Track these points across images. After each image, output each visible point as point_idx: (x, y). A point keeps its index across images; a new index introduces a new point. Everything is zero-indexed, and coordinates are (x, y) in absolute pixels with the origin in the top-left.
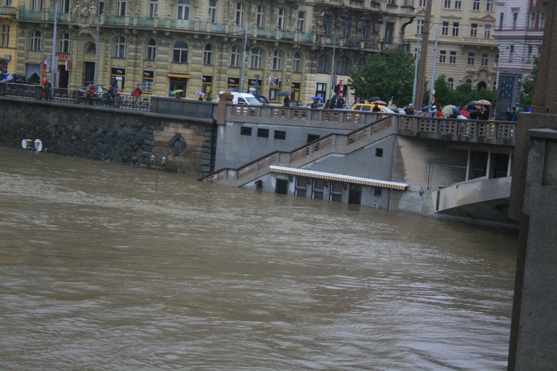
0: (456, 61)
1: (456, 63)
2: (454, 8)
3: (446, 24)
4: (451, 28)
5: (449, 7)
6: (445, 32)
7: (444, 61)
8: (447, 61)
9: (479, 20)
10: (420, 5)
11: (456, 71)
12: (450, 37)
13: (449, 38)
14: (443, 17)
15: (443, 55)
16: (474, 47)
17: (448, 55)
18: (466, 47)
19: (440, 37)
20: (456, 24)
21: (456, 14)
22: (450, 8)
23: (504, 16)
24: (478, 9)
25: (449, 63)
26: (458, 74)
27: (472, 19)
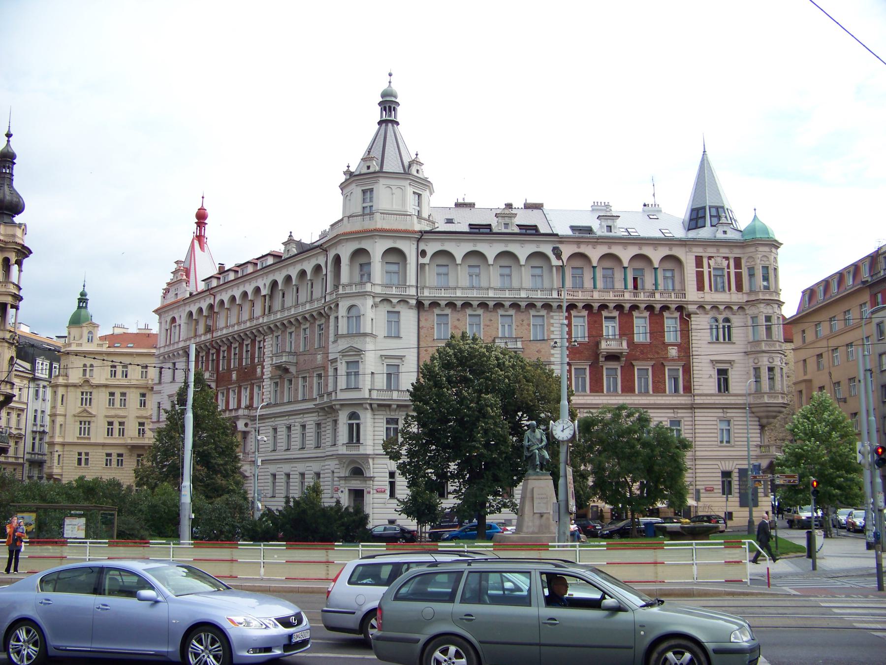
0: (124, 463)
1: (124, 467)
2: (119, 407)
3: (110, 423)
4: (116, 426)
5: (113, 405)
6: (110, 432)
7: (110, 465)
8: (114, 462)
9: (146, 418)
10: (82, 404)
11: (124, 475)
12: (115, 438)
13: (116, 439)
14: (107, 417)
15: (109, 458)
16: (142, 447)
17: (114, 458)
18: (133, 448)
19: (105, 438)
20: (121, 424)
21: (121, 413)
22: (115, 407)
23: (161, 405)
24: (144, 406)
25: (116, 466)
26: (126, 478)
27: (138, 417)
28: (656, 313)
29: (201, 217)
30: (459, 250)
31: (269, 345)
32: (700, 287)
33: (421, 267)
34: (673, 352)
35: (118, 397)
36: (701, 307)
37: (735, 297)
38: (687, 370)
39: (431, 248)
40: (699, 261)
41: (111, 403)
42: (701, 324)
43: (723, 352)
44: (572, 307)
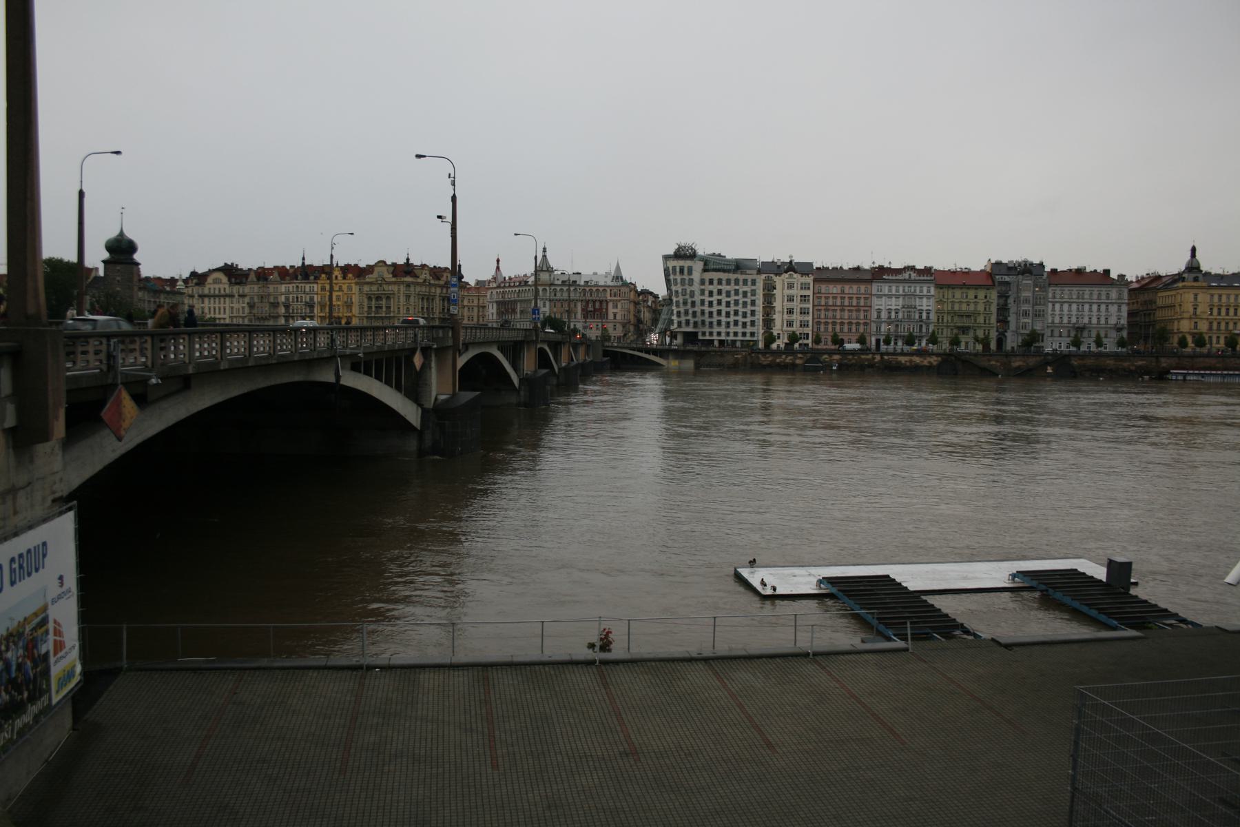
4: (471, 318)
28: (601, 302)
29: (498, 261)
30: (558, 288)
31: (519, 304)
32: (611, 296)
33: (550, 292)
34: (604, 310)
35: (471, 309)
36: (611, 300)
37: (617, 298)
38: (607, 314)
39: (553, 288)
40: (611, 290)
41: (469, 311)
42: (610, 305)
43: (615, 311)
44: (582, 300)
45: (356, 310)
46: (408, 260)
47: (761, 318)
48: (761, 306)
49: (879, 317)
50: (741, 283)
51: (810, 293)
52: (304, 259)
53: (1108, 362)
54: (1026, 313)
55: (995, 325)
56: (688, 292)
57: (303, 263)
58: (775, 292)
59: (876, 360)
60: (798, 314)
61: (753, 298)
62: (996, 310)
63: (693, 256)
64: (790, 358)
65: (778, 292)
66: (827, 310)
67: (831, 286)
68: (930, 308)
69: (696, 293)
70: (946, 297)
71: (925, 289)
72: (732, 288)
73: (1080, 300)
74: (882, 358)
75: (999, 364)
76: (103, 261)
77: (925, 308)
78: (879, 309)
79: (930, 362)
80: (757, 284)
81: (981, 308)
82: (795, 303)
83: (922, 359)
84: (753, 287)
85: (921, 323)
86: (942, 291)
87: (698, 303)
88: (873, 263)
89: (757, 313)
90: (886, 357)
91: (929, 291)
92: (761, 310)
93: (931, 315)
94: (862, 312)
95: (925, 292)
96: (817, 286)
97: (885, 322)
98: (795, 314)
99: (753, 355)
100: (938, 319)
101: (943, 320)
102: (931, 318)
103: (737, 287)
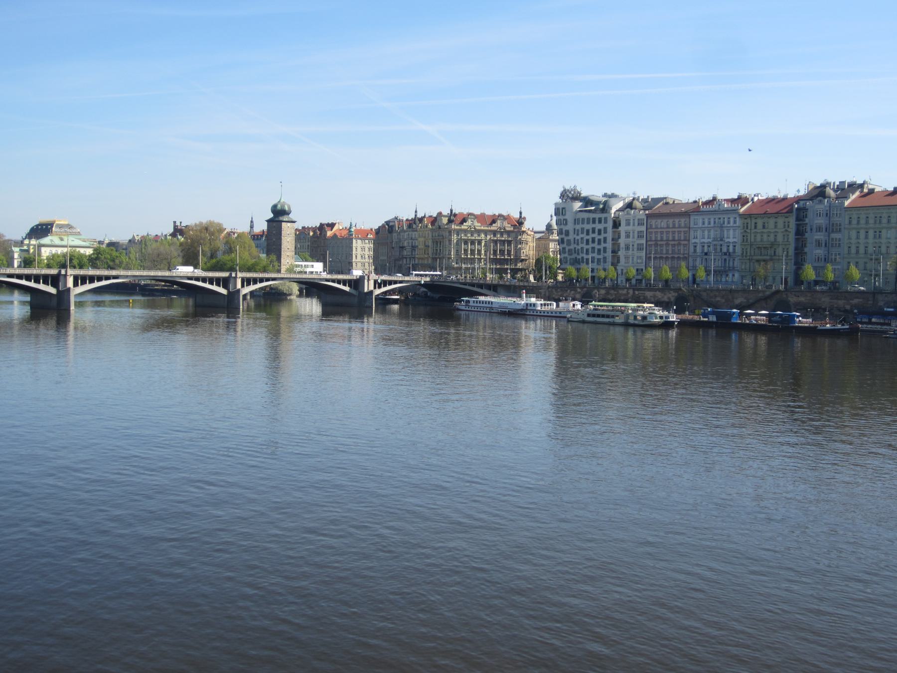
45: (430, 251)
46: (451, 211)
47: (611, 254)
48: (611, 242)
49: (695, 251)
50: (597, 222)
51: (643, 228)
52: (416, 212)
53: (823, 299)
54: (819, 243)
55: (793, 257)
56: (564, 232)
57: (416, 215)
58: (620, 228)
59: (630, 296)
60: (635, 250)
61: (606, 235)
62: (794, 240)
63: (577, 197)
64: (572, 292)
65: (623, 229)
66: (656, 245)
67: (659, 221)
68: (735, 240)
69: (570, 231)
70: (749, 228)
71: (732, 220)
72: (590, 227)
73: (877, 226)
74: (634, 293)
75: (723, 301)
76: (267, 221)
77: (731, 240)
78: (695, 243)
79: (669, 298)
80: (608, 222)
81: (780, 238)
82: (631, 239)
83: (663, 295)
84: (606, 225)
85: (725, 257)
86: (746, 221)
87: (572, 241)
88: (798, 191)
89: (607, 250)
90: (637, 292)
91: (735, 222)
92: (611, 247)
93: (737, 247)
94: (670, 246)
95: (732, 224)
96: (649, 221)
97: (699, 256)
98: (631, 249)
99: (550, 290)
100: (742, 254)
101: (747, 253)
102: (737, 251)
103: (594, 226)
